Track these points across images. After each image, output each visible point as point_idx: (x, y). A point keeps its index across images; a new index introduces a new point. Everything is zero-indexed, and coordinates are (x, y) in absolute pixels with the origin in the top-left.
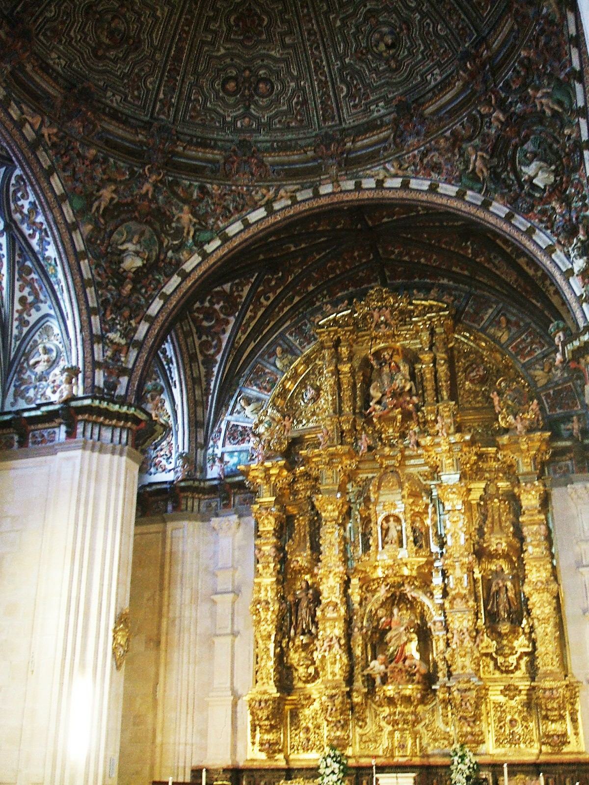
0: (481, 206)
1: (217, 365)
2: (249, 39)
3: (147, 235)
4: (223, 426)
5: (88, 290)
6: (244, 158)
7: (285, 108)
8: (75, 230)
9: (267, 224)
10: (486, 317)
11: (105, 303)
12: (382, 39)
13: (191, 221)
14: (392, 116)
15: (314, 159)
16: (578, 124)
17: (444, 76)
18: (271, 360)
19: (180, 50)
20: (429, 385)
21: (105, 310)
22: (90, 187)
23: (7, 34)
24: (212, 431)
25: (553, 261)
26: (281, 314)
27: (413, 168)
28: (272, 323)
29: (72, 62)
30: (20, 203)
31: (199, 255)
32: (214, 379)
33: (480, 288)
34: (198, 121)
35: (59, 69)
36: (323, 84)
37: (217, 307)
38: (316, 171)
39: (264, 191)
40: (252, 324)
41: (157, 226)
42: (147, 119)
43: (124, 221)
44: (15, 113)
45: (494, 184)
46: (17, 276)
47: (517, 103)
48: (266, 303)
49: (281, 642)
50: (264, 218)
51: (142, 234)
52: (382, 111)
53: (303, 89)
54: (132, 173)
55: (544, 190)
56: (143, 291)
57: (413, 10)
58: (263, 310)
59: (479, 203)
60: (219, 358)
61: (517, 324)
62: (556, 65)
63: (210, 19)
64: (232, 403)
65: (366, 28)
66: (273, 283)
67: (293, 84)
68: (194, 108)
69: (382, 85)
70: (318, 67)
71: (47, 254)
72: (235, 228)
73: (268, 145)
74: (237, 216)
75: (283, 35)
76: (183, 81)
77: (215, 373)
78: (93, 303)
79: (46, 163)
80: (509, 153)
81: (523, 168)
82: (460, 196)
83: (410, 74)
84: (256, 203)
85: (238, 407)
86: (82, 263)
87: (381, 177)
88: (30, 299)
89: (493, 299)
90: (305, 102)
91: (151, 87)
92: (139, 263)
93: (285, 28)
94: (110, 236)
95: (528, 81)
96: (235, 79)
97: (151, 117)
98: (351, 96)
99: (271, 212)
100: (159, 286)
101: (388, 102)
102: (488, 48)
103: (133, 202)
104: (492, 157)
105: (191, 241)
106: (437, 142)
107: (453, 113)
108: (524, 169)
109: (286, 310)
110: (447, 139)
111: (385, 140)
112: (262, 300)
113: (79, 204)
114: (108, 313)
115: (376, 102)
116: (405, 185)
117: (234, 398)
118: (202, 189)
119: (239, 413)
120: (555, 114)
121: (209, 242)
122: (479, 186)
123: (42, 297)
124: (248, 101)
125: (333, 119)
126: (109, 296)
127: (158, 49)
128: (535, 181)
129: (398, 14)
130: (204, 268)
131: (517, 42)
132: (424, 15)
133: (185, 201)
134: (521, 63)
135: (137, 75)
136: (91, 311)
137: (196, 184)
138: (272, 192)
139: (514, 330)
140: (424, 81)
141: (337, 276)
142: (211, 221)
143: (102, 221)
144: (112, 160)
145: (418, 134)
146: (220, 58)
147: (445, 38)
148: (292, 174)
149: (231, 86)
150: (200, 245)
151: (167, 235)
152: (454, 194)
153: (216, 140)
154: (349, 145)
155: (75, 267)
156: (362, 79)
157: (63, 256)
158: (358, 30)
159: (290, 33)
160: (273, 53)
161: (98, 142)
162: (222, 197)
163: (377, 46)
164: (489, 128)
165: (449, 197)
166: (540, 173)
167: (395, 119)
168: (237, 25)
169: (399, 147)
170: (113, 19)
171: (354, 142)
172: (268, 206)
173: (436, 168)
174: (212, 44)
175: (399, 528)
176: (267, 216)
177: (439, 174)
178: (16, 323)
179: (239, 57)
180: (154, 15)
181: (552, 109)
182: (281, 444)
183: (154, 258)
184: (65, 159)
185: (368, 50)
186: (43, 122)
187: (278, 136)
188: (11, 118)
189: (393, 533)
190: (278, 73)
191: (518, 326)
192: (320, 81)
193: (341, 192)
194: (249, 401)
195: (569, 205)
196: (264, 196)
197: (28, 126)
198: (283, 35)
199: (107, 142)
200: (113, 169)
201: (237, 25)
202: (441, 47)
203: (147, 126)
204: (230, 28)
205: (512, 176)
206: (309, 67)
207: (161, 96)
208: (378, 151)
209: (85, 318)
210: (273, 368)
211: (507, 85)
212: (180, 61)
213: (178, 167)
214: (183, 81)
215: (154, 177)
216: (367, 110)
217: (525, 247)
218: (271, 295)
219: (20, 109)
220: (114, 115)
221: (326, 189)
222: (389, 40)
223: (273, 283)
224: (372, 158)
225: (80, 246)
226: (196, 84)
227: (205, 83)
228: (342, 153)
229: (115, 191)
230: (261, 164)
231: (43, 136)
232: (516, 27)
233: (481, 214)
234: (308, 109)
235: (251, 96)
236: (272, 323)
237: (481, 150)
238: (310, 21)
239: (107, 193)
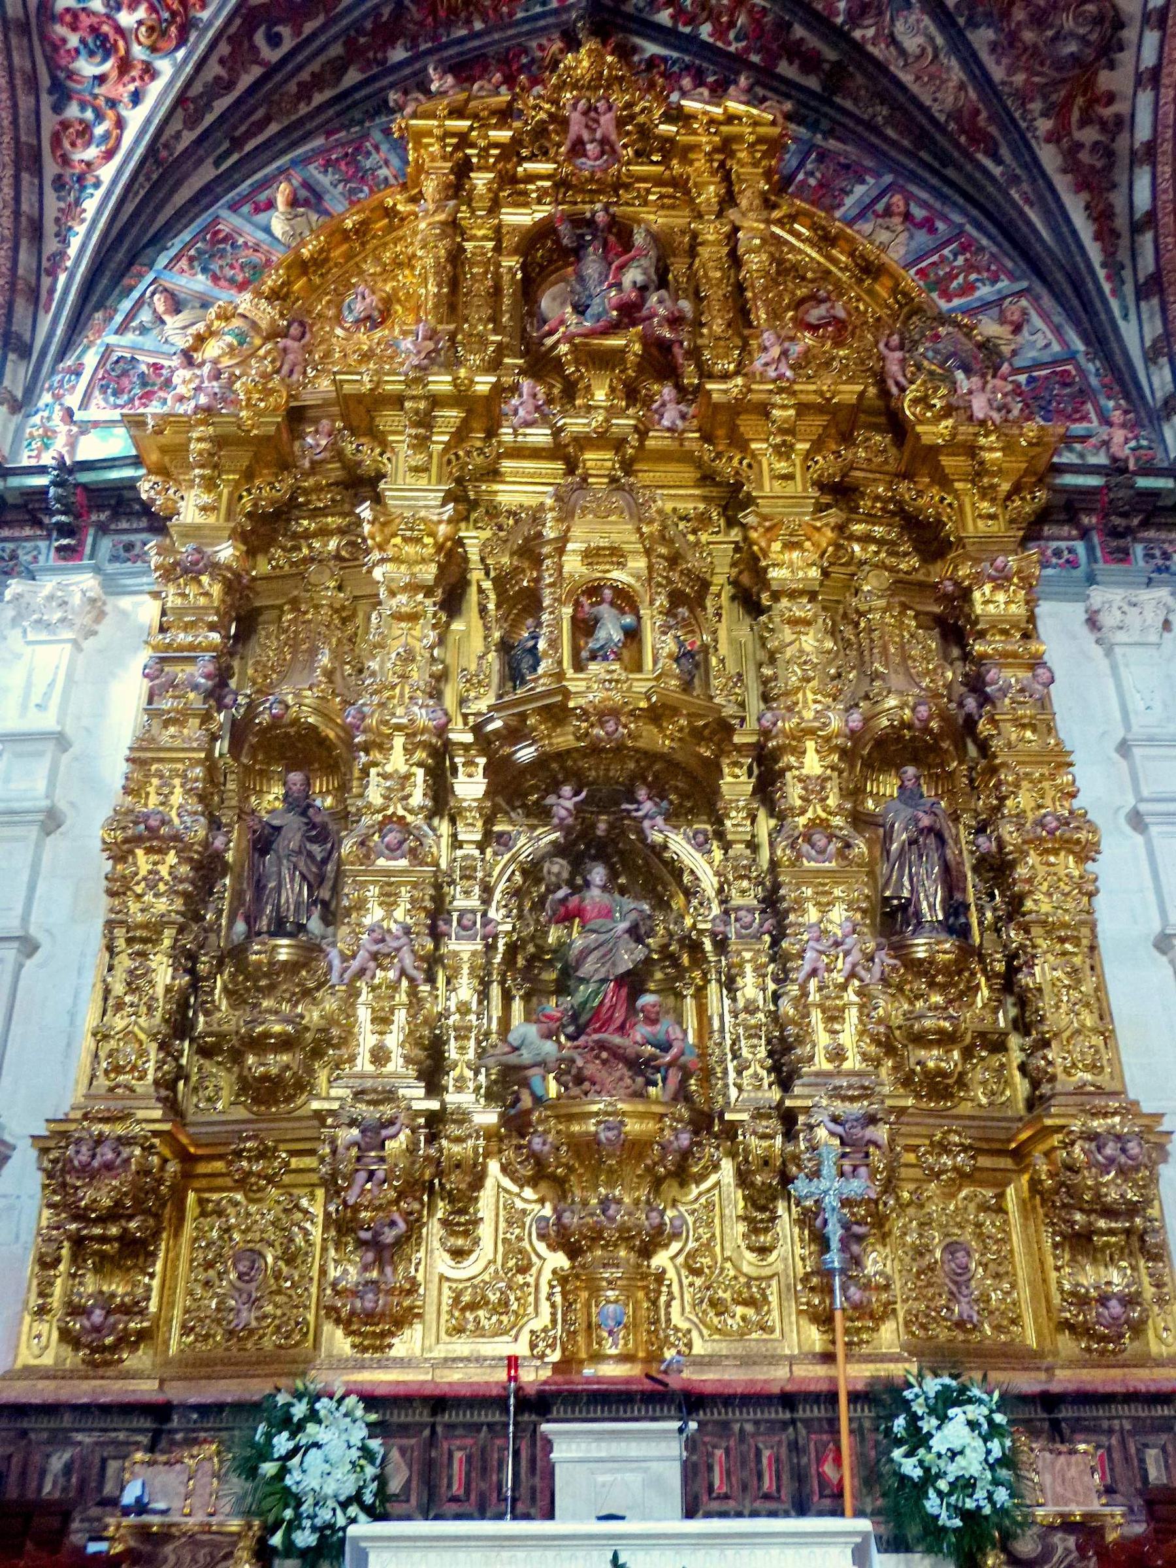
1: (99, 193)
4: (91, 359)
10: (849, 201)
18: (261, 218)
20: (716, 292)
24: (53, 372)
26: (303, 109)
28: (273, 128)
32: (81, 229)
40: (221, 105)
48: (272, 55)
49: (193, 957)
58: (257, 71)
60: (106, 172)
61: (928, 225)
64: (126, 305)
77: (89, 216)
85: (145, 316)
89: (869, 163)
109: (318, 99)
112: (259, 38)
117: (136, 294)
119: (143, 330)
139: (922, 237)
141: (475, 35)
175: (628, 620)
182: (267, 393)
189: (610, 630)
191: (932, 230)
194: (176, 305)
210: (261, 235)
218: (285, 31)
236: (273, 128)
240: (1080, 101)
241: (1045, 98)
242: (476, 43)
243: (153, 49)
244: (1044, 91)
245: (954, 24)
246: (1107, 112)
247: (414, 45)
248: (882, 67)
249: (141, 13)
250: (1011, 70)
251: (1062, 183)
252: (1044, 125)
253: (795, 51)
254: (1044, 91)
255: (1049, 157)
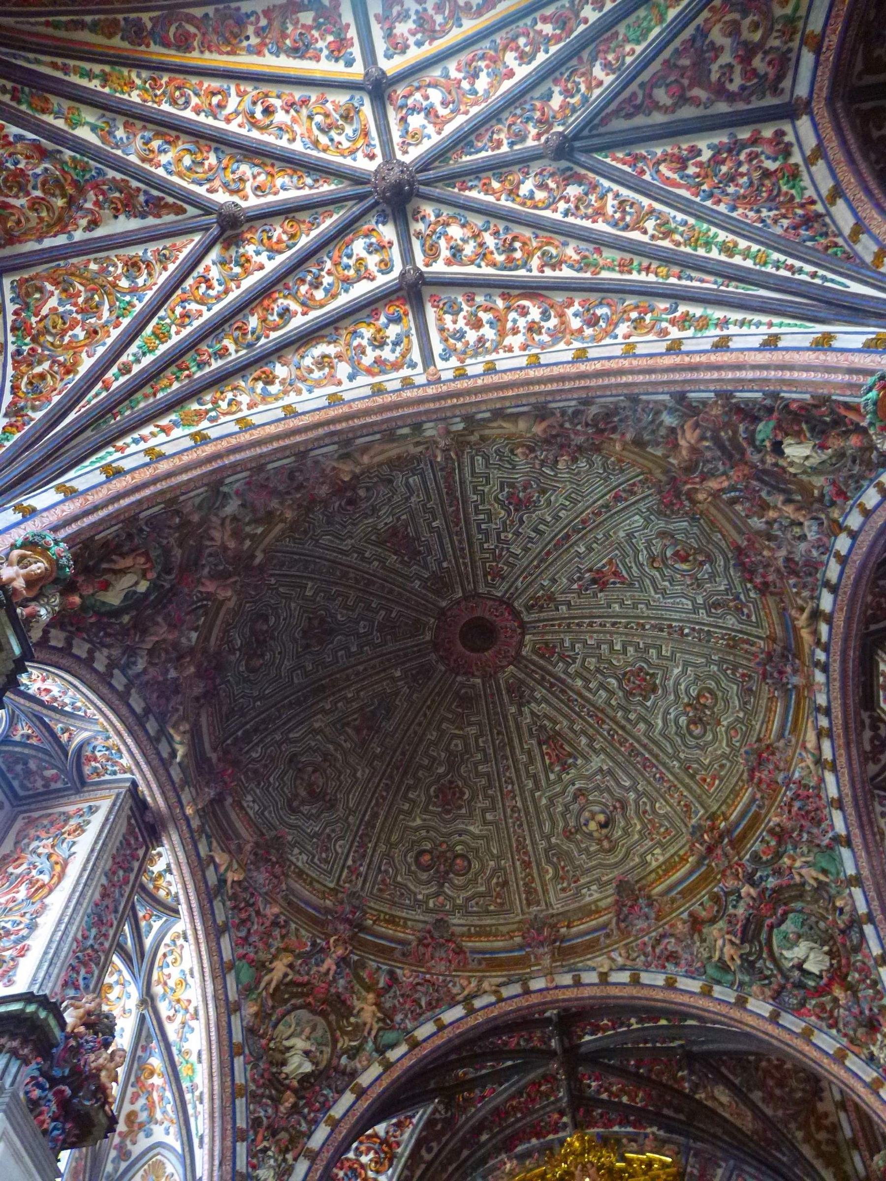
0: (735, 1004)
2: (448, 812)
3: (319, 1032)
5: (237, 1102)
6: (442, 941)
7: (483, 889)
8: (236, 1011)
9: (465, 1027)
11: (256, 1123)
12: (593, 819)
13: (374, 1015)
14: (609, 900)
15: (521, 948)
16: (851, 895)
17: (668, 855)
19: (375, 815)
21: (256, 1134)
22: (263, 956)
23: (219, 759)
25: (848, 1070)
27: (642, 958)
29: (265, 808)
30: (166, 971)
31: (380, 1064)
33: (703, 1141)
34: (386, 895)
35: (251, 813)
36: (527, 865)
37: (364, 1159)
38: (523, 962)
39: (464, 982)
41: (332, 1017)
42: (332, 885)
43: (295, 1008)
44: (203, 850)
45: (749, 974)
46: (132, 1079)
47: (768, 876)
50: (462, 1018)
51: (314, 1029)
52: (596, 896)
53: (504, 869)
54: (314, 944)
55: (820, 977)
56: (306, 1110)
57: (628, 790)
58: (423, 1166)
59: (733, 1000)
62: (815, 831)
63: (409, 788)
65: (575, 807)
66: (439, 1127)
67: (492, 863)
68: (383, 881)
69: (594, 868)
70: (521, 846)
71: (186, 1046)
72: (425, 1030)
73: (465, 929)
74: (429, 1014)
75: (484, 811)
76: (374, 850)
78: (241, 1123)
79: (220, 919)
80: (763, 936)
81: (785, 952)
82: (706, 993)
83: (627, 854)
84: (453, 998)
86: (236, 1060)
87: (605, 969)
88: (143, 1116)
90: (505, 883)
91: (339, 850)
92: (308, 1067)
93: (487, 803)
94: (275, 1026)
95: (781, 850)
96: (429, 852)
97: (338, 884)
98: (556, 877)
99: (471, 1011)
100: (326, 1107)
101: (602, 885)
102: (726, 819)
103: (308, 983)
104: (743, 942)
105: (370, 1044)
106: (672, 926)
107: (689, 892)
108: (787, 954)
109: (450, 1169)
110: (685, 922)
111: (604, 926)
113: (247, 974)
114: (260, 1137)
115: (588, 885)
116: (635, 981)
118: (392, 974)
120: (821, 885)
121: (392, 1046)
122: (730, 977)
123: (159, 1115)
124: (442, 879)
125: (538, 904)
126: (262, 1114)
127: (352, 812)
128: (805, 966)
129: (611, 793)
130: (385, 1082)
131: (763, 811)
132: (639, 795)
133: (368, 989)
134: (771, 832)
135: (329, 836)
136: (239, 1135)
137: (384, 967)
138: (474, 984)
140: (644, 863)
141: (518, 1120)
142: (398, 1018)
143: (270, 1003)
144: (293, 926)
145: (647, 918)
146: (417, 829)
147: (666, 816)
148: (493, 963)
149: (426, 858)
150: (381, 1050)
151: (344, 1033)
152: (698, 990)
153: (406, 919)
154: (563, 930)
155: (227, 1064)
156: (572, 860)
157: (214, 1047)
158: (566, 807)
159: (494, 809)
160: (472, 828)
161: (281, 901)
162: (414, 987)
163: (586, 825)
164: (735, 907)
165: (692, 993)
166: (812, 956)
167: (617, 902)
168: (437, 797)
169: (625, 933)
170: (314, 772)
171: (568, 927)
172: (468, 1001)
173: (673, 957)
174: (409, 813)
176: (466, 1016)
177: (677, 964)
178: (113, 1154)
179: (436, 830)
180: (354, 775)
181: (816, 879)
183: (324, 1063)
184: (243, 915)
185: (578, 830)
186: (229, 867)
187: (476, 921)
188: (198, 855)
190: (477, 850)
192: (524, 862)
193: (557, 987)
195: (855, 993)
196: (463, 988)
197: (212, 868)
198: (484, 811)
199: (290, 903)
200: (294, 938)
201: (437, 797)
202: (661, 825)
203: (335, 891)
204: (429, 798)
205: (768, 964)
206: (511, 846)
207: (350, 862)
208: (597, 940)
209: (229, 1143)
211: (756, 858)
212: (374, 827)
213: (363, 945)
214: (374, 850)
215: (340, 952)
216: (578, 894)
217: (805, 1055)
219: (210, 845)
220: (300, 873)
221: (537, 984)
222: (601, 818)
223: (439, 1127)
224: (591, 947)
225: (238, 1037)
226: (387, 855)
227: (397, 853)
228: (555, 941)
229: (291, 966)
230: (460, 951)
231: (225, 881)
232: (758, 796)
233: (736, 1014)
234: (509, 892)
235: (447, 873)
237: (728, 933)
238: (514, 798)
239: (280, 968)
240: (812, 1120)
241: (796, 1121)
242: (520, 1124)
243: (378, 1172)
244: (794, 1117)
245: (740, 1090)
246: (826, 1122)
247: (491, 1130)
248: (713, 1112)
249: (371, 1155)
250: (775, 1110)
251: (818, 1164)
252: (800, 1135)
253: (669, 1105)
254: (794, 1117)
255: (807, 1151)
